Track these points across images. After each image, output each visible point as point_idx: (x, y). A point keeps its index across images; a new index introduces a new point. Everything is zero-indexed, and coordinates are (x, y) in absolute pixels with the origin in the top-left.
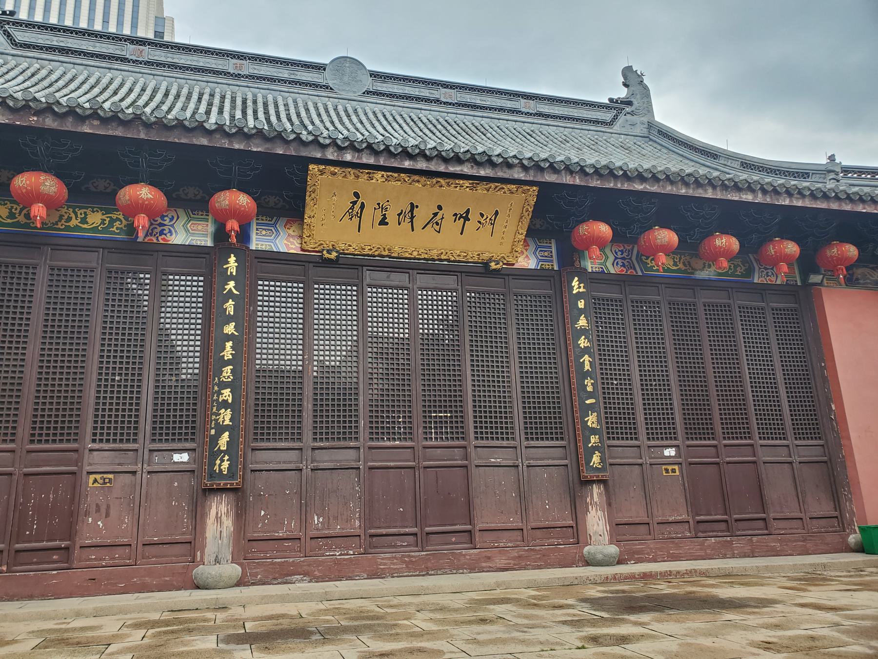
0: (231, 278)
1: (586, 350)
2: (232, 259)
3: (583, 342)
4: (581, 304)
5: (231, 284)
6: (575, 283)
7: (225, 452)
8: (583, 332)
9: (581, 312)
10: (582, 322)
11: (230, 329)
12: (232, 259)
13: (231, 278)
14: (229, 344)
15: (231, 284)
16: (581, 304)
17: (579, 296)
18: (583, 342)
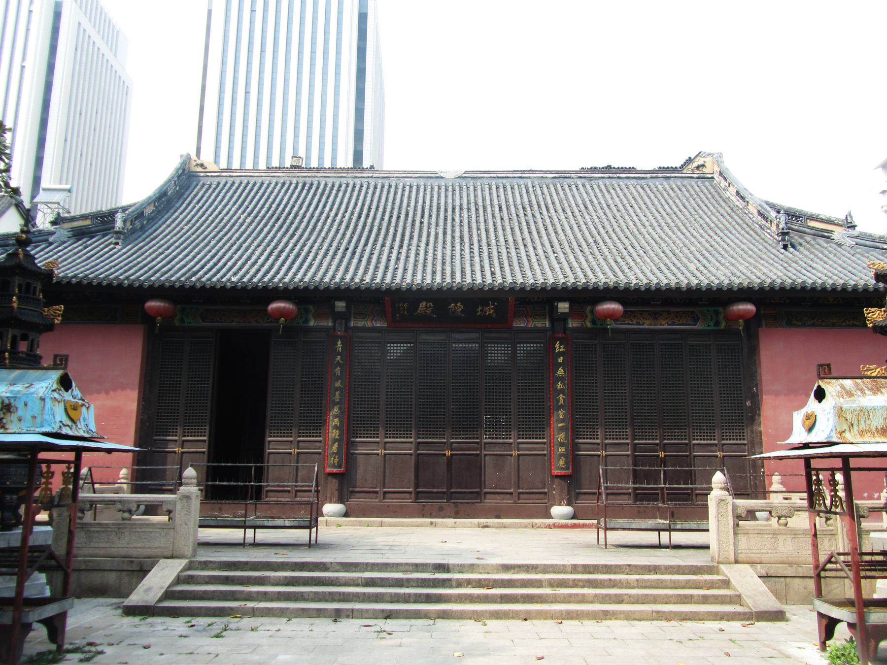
0: (339, 354)
1: (562, 391)
2: (339, 343)
3: (559, 386)
4: (560, 360)
5: (339, 358)
6: (557, 345)
7: (336, 454)
8: (561, 379)
9: (560, 365)
10: (561, 372)
11: (338, 384)
12: (339, 343)
13: (339, 354)
14: (337, 393)
15: (339, 358)
16: (560, 360)
17: (560, 354)
18: (559, 386)
